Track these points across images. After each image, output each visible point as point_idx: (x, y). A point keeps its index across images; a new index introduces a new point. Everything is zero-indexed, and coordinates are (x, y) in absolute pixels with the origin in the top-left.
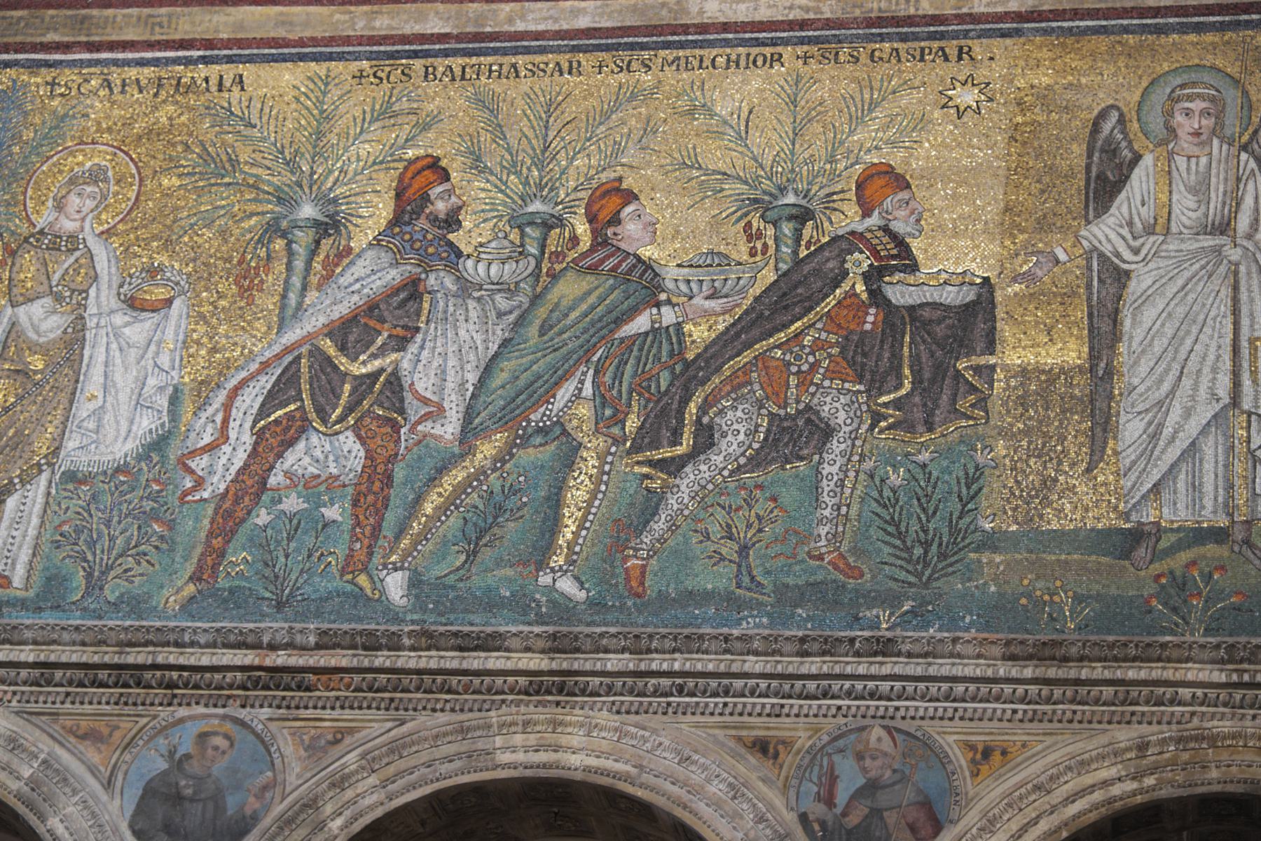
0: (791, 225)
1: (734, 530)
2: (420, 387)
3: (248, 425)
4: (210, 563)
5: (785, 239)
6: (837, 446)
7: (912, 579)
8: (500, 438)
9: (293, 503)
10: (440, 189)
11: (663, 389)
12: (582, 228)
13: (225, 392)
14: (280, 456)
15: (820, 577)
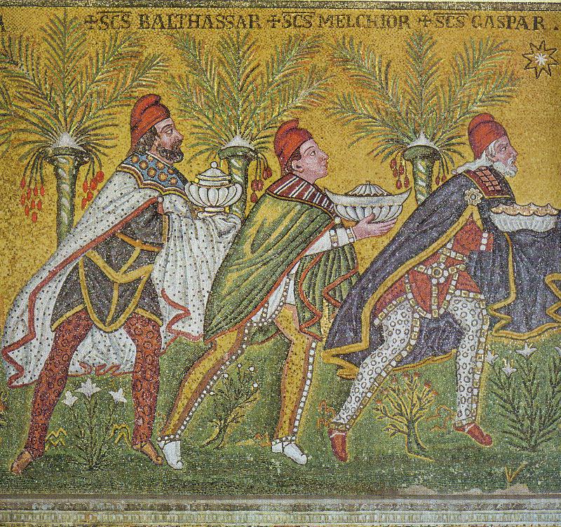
0: (424, 163)
1: (403, 408)
2: (169, 293)
3: (48, 323)
4: (37, 435)
5: (420, 174)
6: (468, 342)
7: (524, 444)
8: (233, 336)
9: (89, 388)
10: (162, 124)
11: (344, 297)
12: (274, 163)
13: (28, 296)
14: (74, 348)
15: (462, 443)
